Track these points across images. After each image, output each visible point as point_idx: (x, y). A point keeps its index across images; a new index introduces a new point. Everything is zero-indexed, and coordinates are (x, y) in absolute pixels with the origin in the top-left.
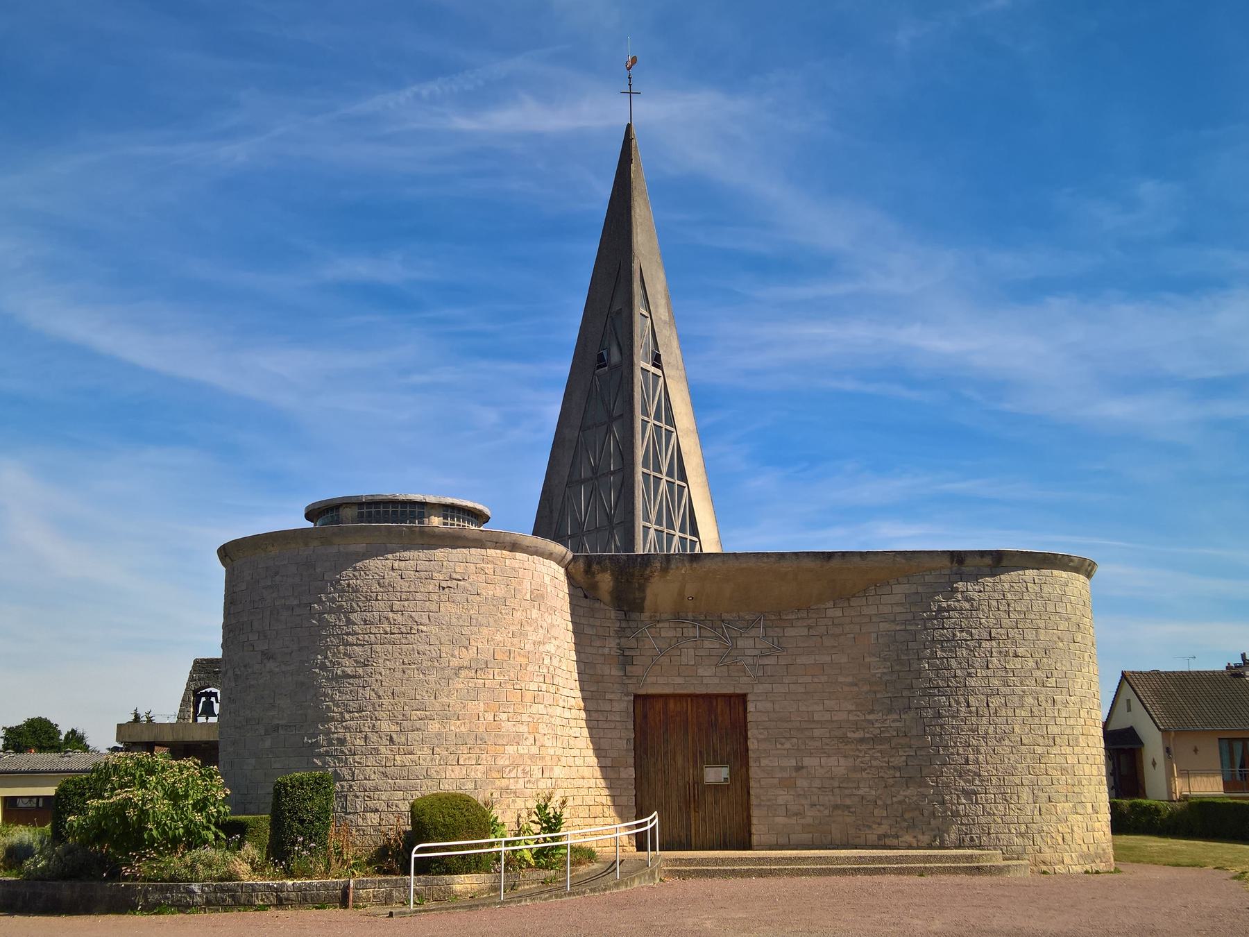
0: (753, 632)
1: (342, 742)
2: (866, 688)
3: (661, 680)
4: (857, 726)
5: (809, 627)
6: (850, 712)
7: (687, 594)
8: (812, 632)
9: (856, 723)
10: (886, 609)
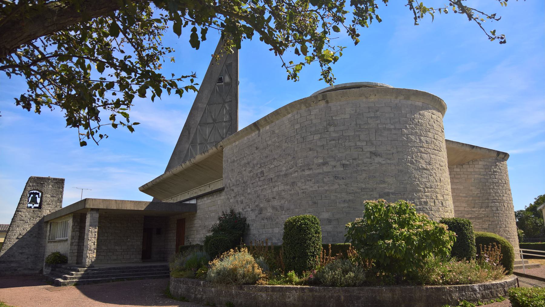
1: (426, 203)
2: (471, 198)
6: (465, 207)
9: (468, 211)
10: (477, 170)
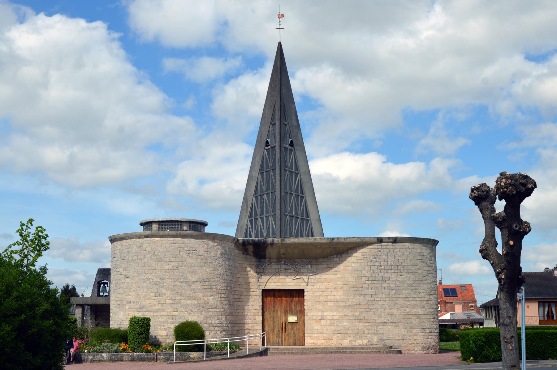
0: (307, 266)
3: (272, 284)
4: (343, 301)
5: (327, 264)
7: (281, 253)
8: (329, 266)
